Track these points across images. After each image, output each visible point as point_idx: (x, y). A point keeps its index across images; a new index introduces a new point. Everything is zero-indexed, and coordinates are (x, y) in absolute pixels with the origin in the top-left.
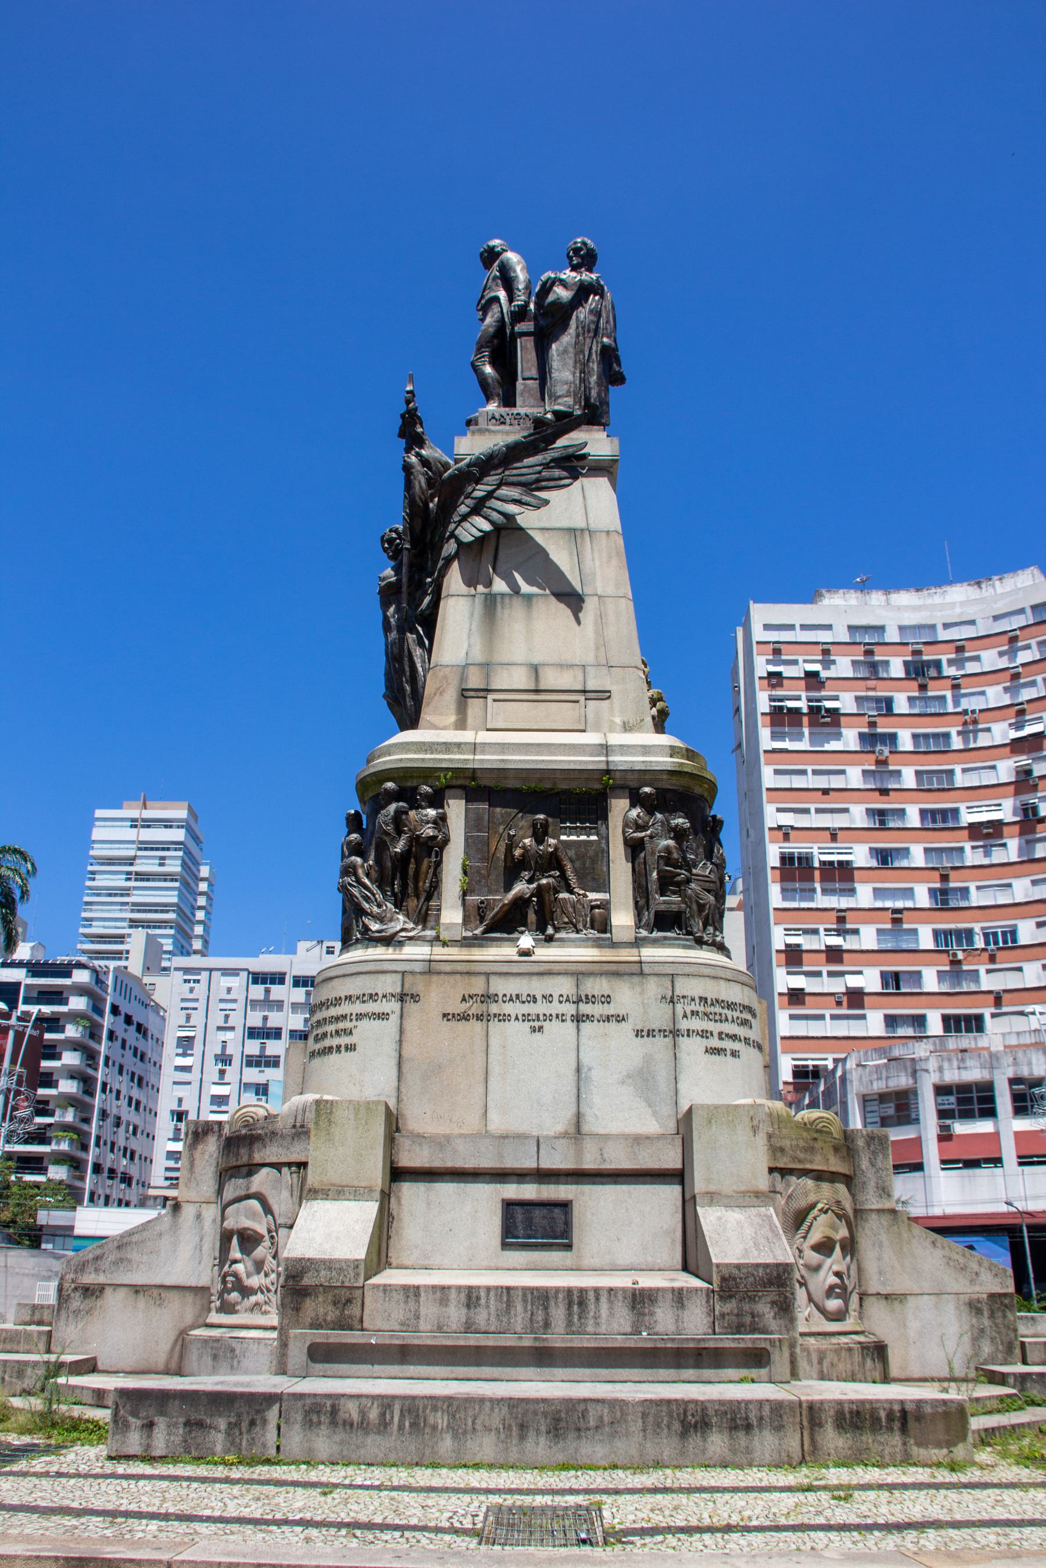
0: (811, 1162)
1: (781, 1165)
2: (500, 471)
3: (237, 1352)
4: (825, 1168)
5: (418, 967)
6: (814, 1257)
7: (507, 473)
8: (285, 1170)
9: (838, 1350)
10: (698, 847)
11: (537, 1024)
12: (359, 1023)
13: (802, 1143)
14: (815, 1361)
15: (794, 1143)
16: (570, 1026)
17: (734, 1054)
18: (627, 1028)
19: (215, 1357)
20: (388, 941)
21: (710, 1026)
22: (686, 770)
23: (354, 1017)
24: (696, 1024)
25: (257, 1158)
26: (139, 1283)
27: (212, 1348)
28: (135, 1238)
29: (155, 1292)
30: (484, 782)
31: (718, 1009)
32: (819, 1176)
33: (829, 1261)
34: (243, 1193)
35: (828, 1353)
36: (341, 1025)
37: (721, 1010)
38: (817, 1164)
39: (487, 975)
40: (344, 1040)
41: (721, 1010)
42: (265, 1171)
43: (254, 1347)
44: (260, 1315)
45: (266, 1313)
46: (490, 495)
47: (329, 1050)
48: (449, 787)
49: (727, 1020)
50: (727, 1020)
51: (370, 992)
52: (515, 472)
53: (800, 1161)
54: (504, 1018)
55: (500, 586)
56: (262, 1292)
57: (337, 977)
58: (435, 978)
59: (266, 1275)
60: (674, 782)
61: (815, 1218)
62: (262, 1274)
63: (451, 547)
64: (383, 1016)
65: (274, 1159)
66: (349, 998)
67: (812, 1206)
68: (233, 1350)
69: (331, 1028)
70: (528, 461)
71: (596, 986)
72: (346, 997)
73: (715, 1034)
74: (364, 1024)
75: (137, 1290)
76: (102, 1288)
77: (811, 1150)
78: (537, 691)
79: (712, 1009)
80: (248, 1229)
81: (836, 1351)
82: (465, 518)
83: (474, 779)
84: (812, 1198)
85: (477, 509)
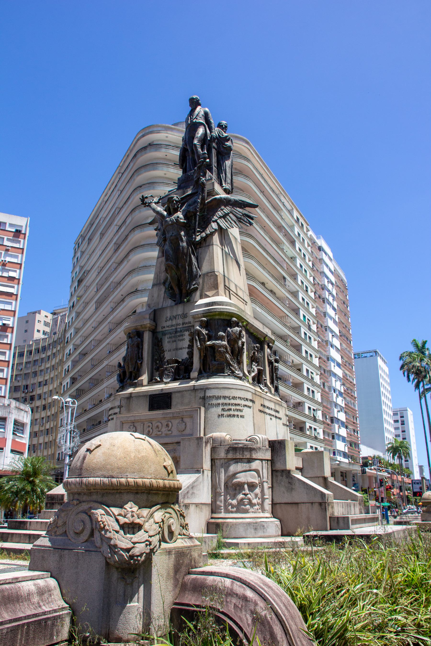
2: (231, 207)
3: (265, 526)
5: (254, 391)
7: (233, 209)
8: (264, 462)
11: (271, 417)
12: (244, 408)
16: (275, 418)
18: (281, 422)
19: (256, 529)
20: (240, 378)
23: (242, 405)
25: (254, 456)
26: (197, 503)
27: (253, 526)
28: (195, 484)
29: (200, 506)
34: (248, 469)
36: (238, 407)
39: (264, 398)
40: (240, 413)
42: (257, 462)
43: (271, 524)
44: (258, 514)
45: (259, 512)
46: (228, 214)
47: (234, 416)
51: (246, 397)
52: (235, 210)
54: (267, 414)
56: (258, 505)
57: (232, 388)
58: (257, 396)
59: (259, 499)
62: (257, 498)
63: (214, 226)
64: (250, 407)
65: (261, 458)
66: (240, 398)
68: (263, 526)
69: (233, 408)
70: (238, 209)
71: (278, 408)
72: (239, 397)
74: (246, 409)
75: (197, 505)
76: (189, 504)
78: (237, 295)
80: (254, 482)
82: (220, 217)
85: (224, 217)
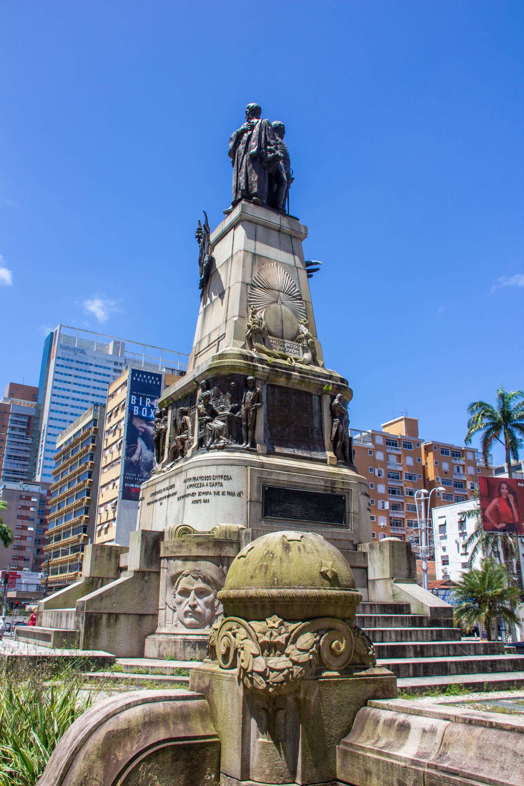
0: (180, 552)
1: (166, 555)
4: (189, 555)
6: (179, 598)
9: (168, 642)
10: (226, 400)
13: (176, 544)
14: (157, 646)
15: (172, 544)
17: (206, 501)
18: (176, 497)
21: (196, 490)
22: (212, 367)
24: (191, 491)
30: (175, 399)
31: (200, 481)
32: (186, 559)
33: (187, 600)
35: (163, 643)
37: (202, 482)
38: (184, 553)
41: (202, 482)
48: (169, 406)
49: (203, 485)
50: (203, 485)
53: (174, 553)
55: (209, 302)
60: (211, 374)
61: (181, 579)
67: (179, 574)
73: (197, 494)
77: (181, 546)
79: (197, 482)
81: (167, 642)
83: (172, 399)
84: (179, 570)
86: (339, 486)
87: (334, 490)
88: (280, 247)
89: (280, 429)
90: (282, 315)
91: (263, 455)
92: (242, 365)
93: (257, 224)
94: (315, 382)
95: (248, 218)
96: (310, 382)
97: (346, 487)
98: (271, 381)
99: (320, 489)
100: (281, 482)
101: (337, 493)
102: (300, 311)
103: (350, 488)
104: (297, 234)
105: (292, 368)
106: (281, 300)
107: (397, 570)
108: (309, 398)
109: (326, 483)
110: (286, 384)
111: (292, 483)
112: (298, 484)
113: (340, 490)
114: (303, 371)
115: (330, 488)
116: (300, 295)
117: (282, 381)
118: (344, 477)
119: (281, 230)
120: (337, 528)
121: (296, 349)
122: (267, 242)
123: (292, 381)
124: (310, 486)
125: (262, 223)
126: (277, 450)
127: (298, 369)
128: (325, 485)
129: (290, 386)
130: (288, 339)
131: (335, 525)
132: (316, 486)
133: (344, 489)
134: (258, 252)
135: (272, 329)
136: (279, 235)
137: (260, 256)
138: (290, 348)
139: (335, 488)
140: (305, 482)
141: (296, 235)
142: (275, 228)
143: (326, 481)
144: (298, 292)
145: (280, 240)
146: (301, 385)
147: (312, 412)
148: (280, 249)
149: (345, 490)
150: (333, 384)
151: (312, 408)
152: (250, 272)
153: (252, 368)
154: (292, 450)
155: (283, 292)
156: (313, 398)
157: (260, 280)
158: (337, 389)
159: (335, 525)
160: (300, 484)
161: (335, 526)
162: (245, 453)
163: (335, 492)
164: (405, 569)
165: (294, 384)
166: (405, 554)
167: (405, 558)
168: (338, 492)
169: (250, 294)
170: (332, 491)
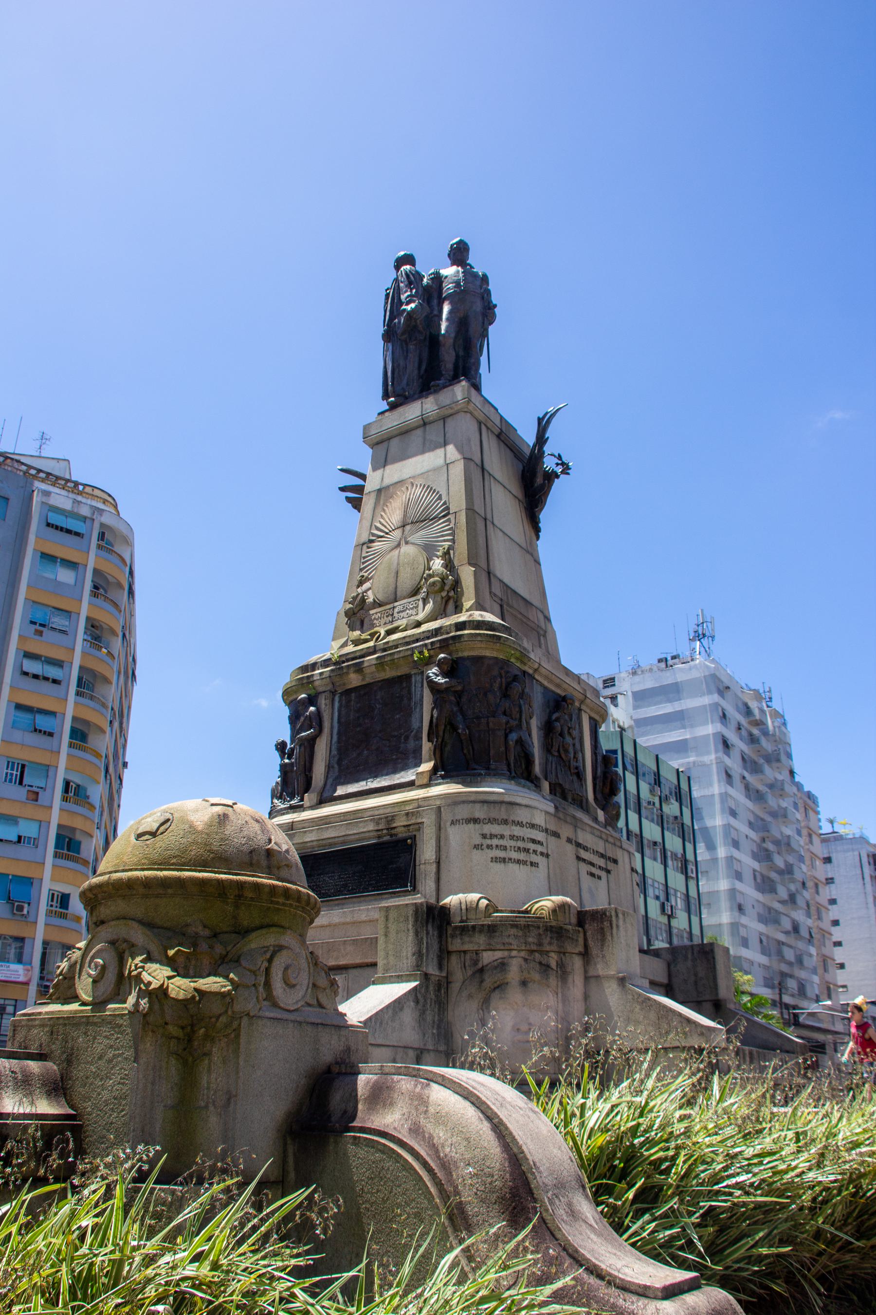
86: (400, 822)
87: (393, 832)
88: (426, 447)
89: (355, 755)
90: (398, 564)
91: (312, 808)
92: (294, 684)
93: (389, 439)
94: (402, 655)
95: (375, 441)
96: (393, 660)
97: (413, 822)
98: (339, 686)
99: (370, 838)
100: (309, 844)
101: (400, 835)
102: (442, 536)
103: (419, 820)
104: (451, 408)
105: (371, 650)
106: (405, 538)
107: (391, 958)
108: (404, 685)
109: (378, 824)
110: (363, 680)
111: (324, 842)
112: (333, 840)
113: (403, 829)
114: (390, 644)
115: (385, 831)
116: (448, 508)
117: (354, 680)
118: (421, 803)
119: (426, 421)
120: (400, 896)
121: (412, 609)
122: (404, 456)
123: (367, 671)
124: (353, 837)
125: (396, 433)
126: (340, 791)
127: (382, 647)
128: (376, 828)
129: (368, 680)
130: (404, 598)
131: (394, 893)
132: (363, 835)
133: (410, 825)
134: (387, 481)
135: (381, 597)
136: (425, 431)
137: (388, 487)
138: (402, 612)
139: (395, 828)
140: (344, 834)
141: (450, 411)
142: (417, 424)
143: (377, 822)
144: (445, 503)
145: (424, 439)
146: (384, 670)
147: (409, 705)
148: (423, 452)
149: (411, 827)
150: (432, 643)
151: (410, 699)
152: (368, 524)
153: (305, 681)
154: (364, 783)
155: (412, 523)
156: (413, 680)
157: (383, 525)
158: (440, 648)
159: (394, 893)
160: (337, 840)
161: (395, 895)
162: (288, 813)
163: (396, 835)
164: (410, 954)
165: (372, 675)
166: (410, 926)
167: (411, 933)
168: (402, 833)
169: (364, 558)
170: (391, 836)
